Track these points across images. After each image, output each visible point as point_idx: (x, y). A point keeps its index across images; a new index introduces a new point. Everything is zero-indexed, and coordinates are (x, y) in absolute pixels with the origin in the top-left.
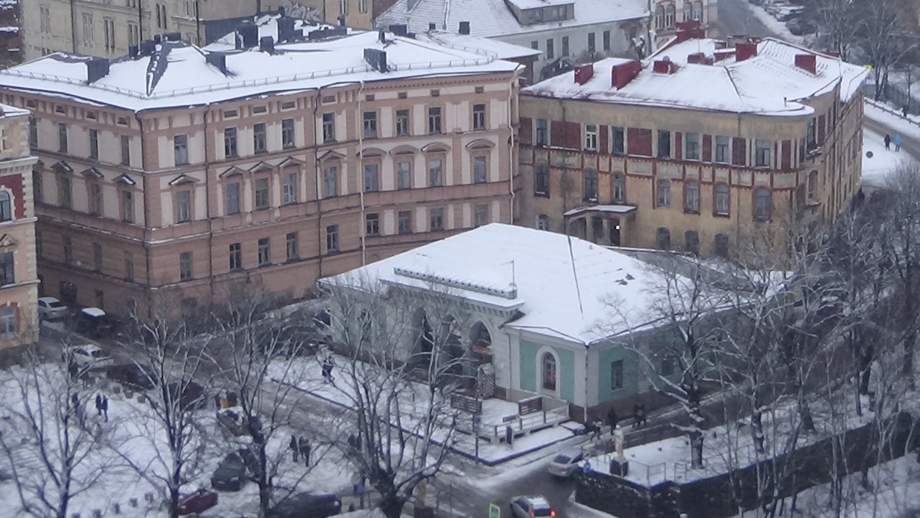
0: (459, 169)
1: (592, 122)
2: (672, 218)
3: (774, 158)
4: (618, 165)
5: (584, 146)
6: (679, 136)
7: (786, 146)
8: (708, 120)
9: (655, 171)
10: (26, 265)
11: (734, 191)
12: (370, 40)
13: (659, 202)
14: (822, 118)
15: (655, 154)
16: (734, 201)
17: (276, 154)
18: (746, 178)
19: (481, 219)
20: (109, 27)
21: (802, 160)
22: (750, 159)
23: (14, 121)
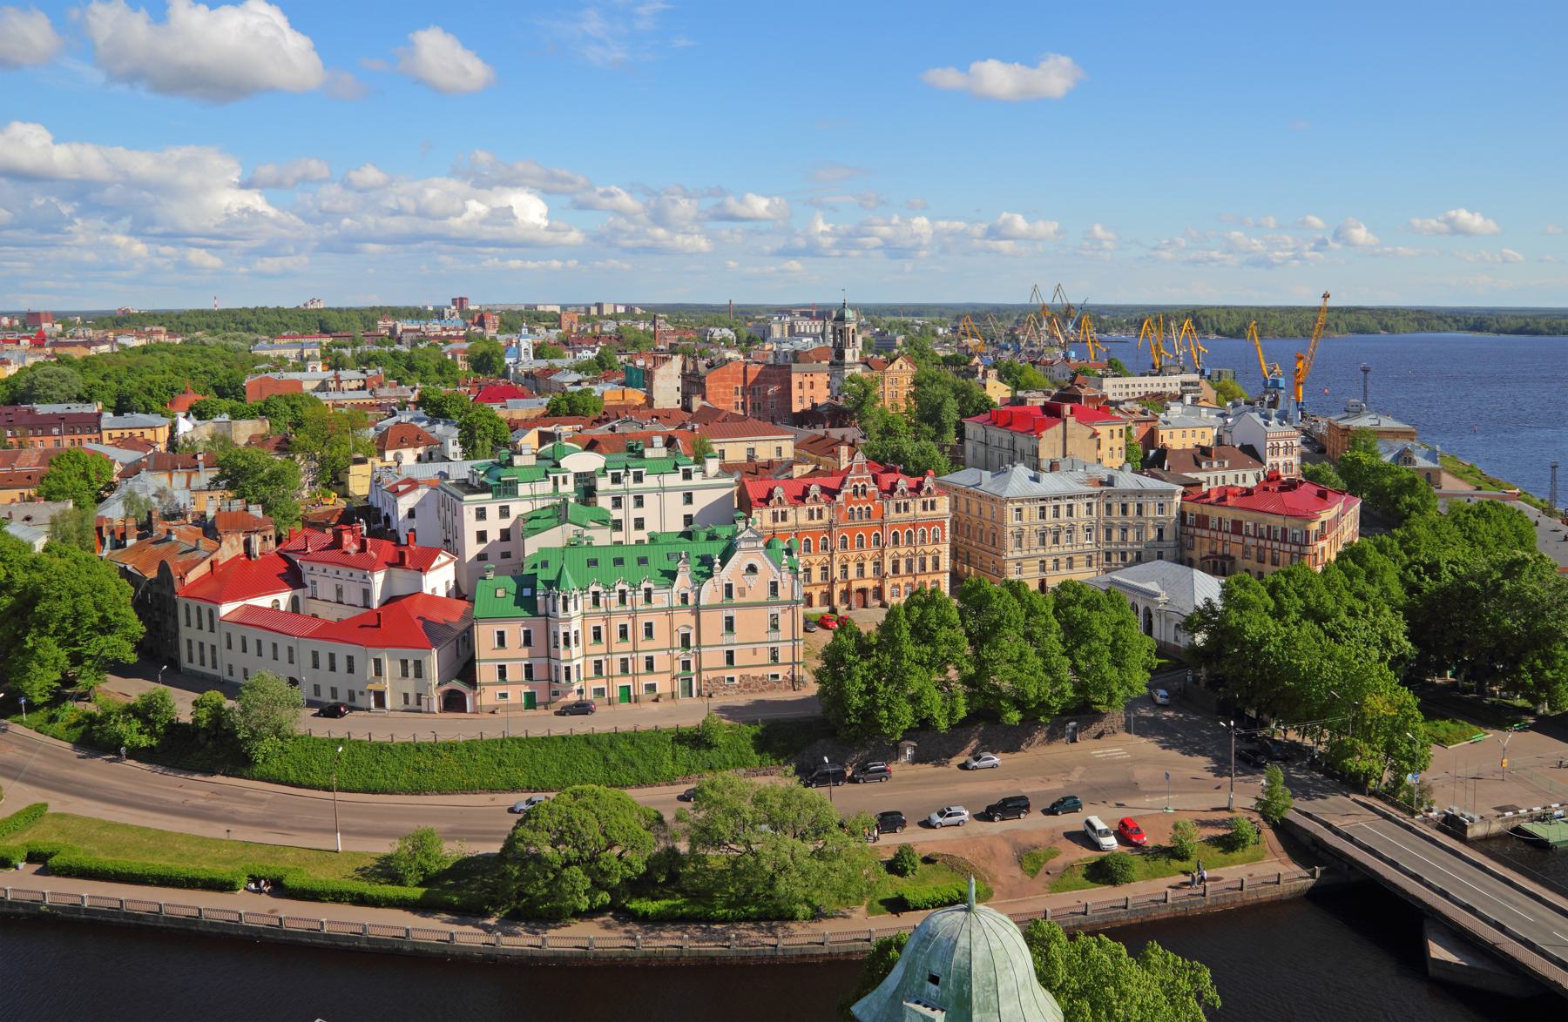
2: (1251, 563)
10: (945, 563)
18: (1287, 547)
19: (1160, 557)
22: (1289, 536)
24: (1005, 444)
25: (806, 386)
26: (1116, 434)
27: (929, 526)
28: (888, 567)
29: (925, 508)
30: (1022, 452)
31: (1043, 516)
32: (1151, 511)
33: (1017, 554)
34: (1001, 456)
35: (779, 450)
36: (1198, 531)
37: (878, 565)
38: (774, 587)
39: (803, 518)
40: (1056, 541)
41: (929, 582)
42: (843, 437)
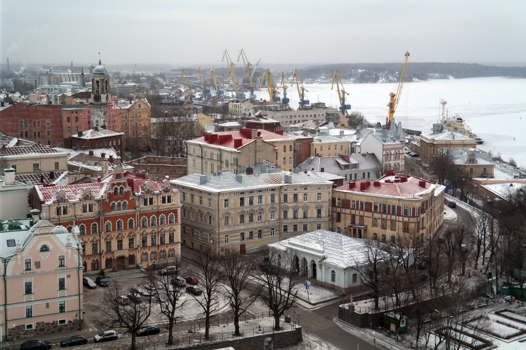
0: (312, 213)
1: (354, 199)
2: (378, 230)
3: (410, 213)
4: (362, 213)
5: (351, 207)
6: (380, 205)
7: (414, 209)
8: (388, 201)
9: (373, 215)
10: (178, 237)
11: (397, 222)
12: (288, 173)
13: (374, 225)
14: (427, 201)
15: (373, 210)
16: (397, 226)
17: (256, 206)
19: (319, 228)
20: (212, 165)
21: (419, 214)
23: (176, 194)
24: (215, 157)
25: (73, 120)
26: (288, 148)
27: (166, 213)
28: (138, 241)
29: (164, 202)
30: (227, 162)
31: (242, 203)
32: (312, 196)
33: (226, 229)
34: (212, 165)
35: (57, 164)
36: (343, 210)
37: (131, 241)
38: (62, 259)
39: (79, 212)
40: (251, 220)
41: (167, 250)
42: (103, 155)
